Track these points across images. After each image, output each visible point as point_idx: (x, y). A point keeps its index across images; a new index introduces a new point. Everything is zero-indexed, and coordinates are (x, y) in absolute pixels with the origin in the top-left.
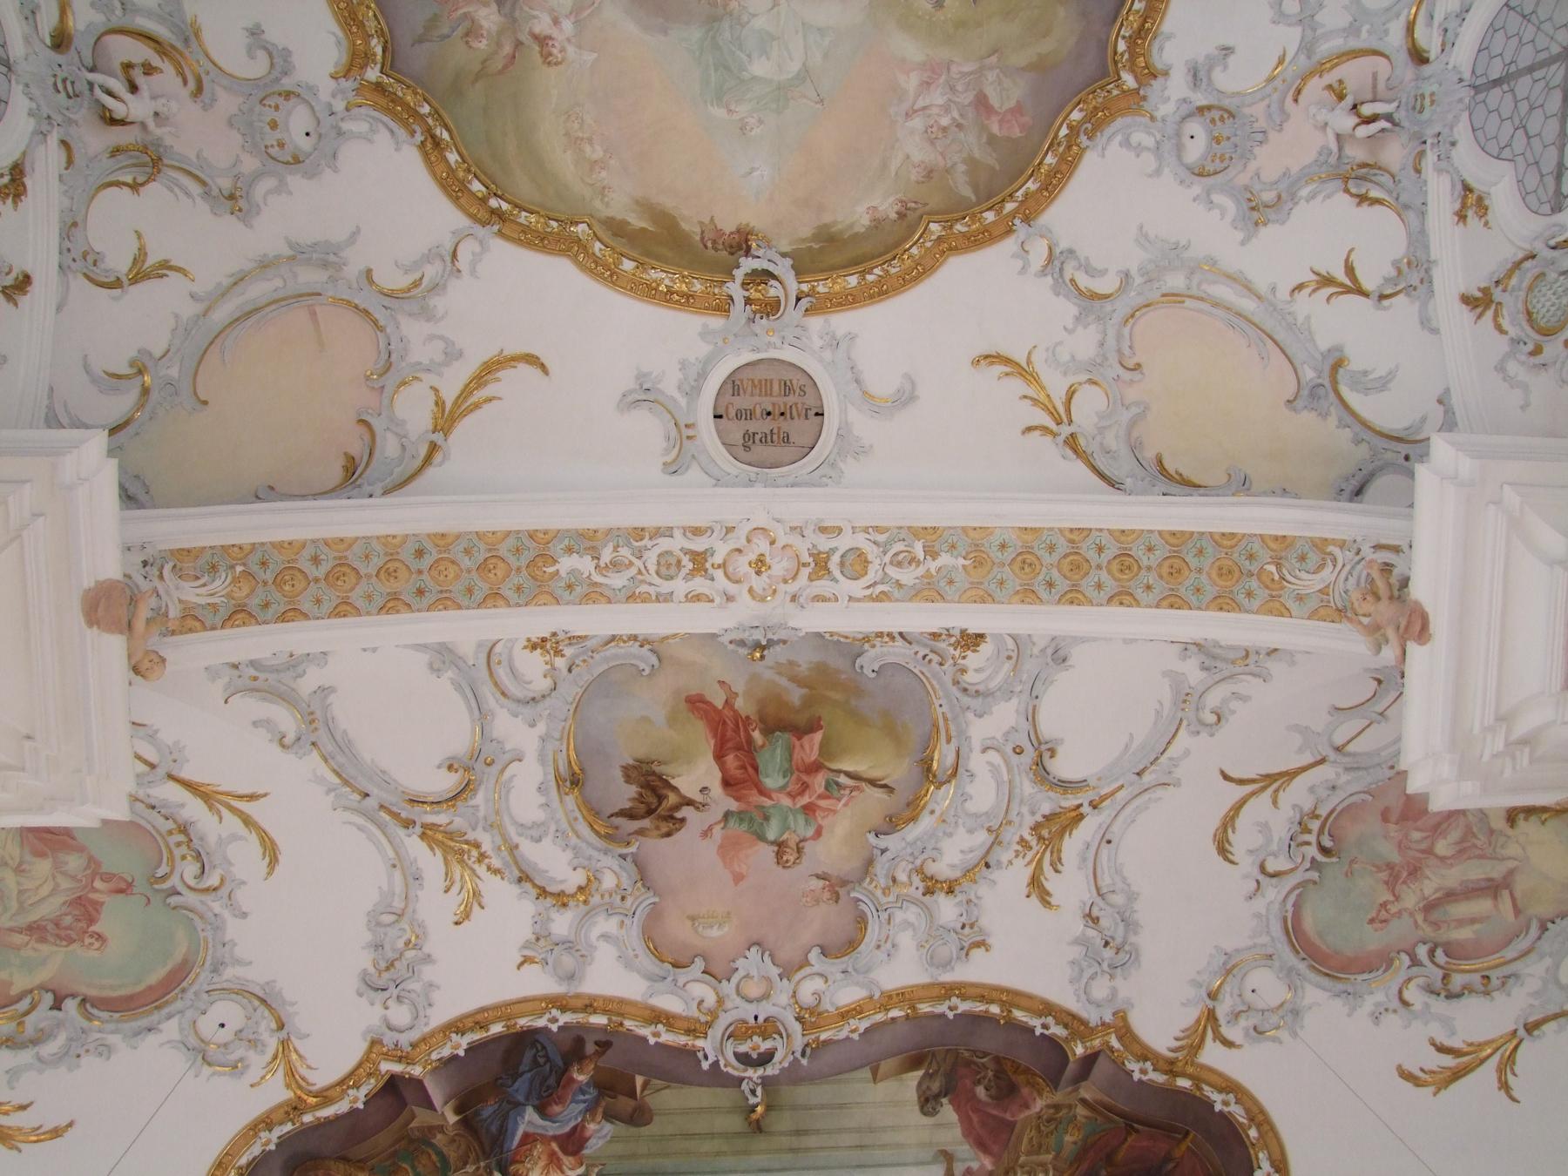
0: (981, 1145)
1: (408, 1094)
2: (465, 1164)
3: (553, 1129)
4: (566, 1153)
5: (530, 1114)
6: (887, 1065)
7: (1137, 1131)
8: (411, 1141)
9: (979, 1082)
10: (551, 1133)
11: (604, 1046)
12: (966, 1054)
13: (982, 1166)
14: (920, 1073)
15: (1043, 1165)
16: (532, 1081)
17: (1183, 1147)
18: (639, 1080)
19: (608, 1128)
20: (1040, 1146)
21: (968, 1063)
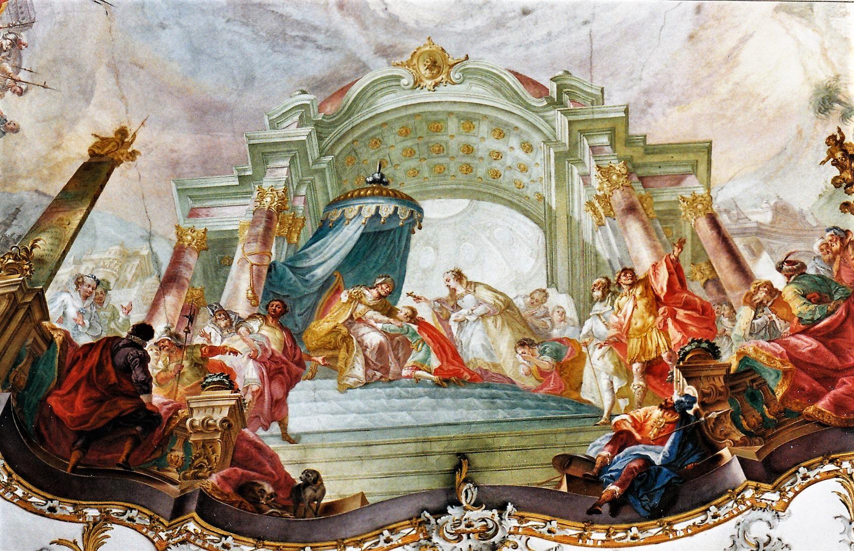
0: (261, 449)
1: (760, 470)
2: (718, 418)
3: (640, 449)
4: (629, 433)
5: (657, 459)
6: (357, 505)
7: (119, 465)
8: (762, 435)
9: (271, 495)
10: (641, 446)
11: (594, 510)
12: (288, 515)
13: (254, 431)
14: (323, 502)
15: (197, 432)
16: (654, 485)
17: (73, 460)
18: (564, 488)
19: (592, 453)
20: (204, 446)
21: (285, 508)
